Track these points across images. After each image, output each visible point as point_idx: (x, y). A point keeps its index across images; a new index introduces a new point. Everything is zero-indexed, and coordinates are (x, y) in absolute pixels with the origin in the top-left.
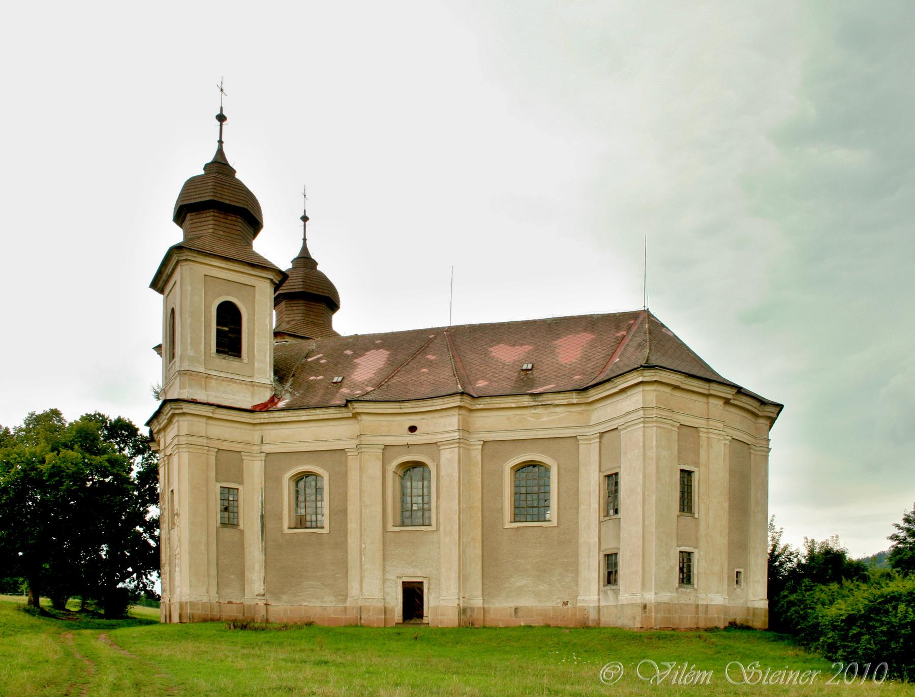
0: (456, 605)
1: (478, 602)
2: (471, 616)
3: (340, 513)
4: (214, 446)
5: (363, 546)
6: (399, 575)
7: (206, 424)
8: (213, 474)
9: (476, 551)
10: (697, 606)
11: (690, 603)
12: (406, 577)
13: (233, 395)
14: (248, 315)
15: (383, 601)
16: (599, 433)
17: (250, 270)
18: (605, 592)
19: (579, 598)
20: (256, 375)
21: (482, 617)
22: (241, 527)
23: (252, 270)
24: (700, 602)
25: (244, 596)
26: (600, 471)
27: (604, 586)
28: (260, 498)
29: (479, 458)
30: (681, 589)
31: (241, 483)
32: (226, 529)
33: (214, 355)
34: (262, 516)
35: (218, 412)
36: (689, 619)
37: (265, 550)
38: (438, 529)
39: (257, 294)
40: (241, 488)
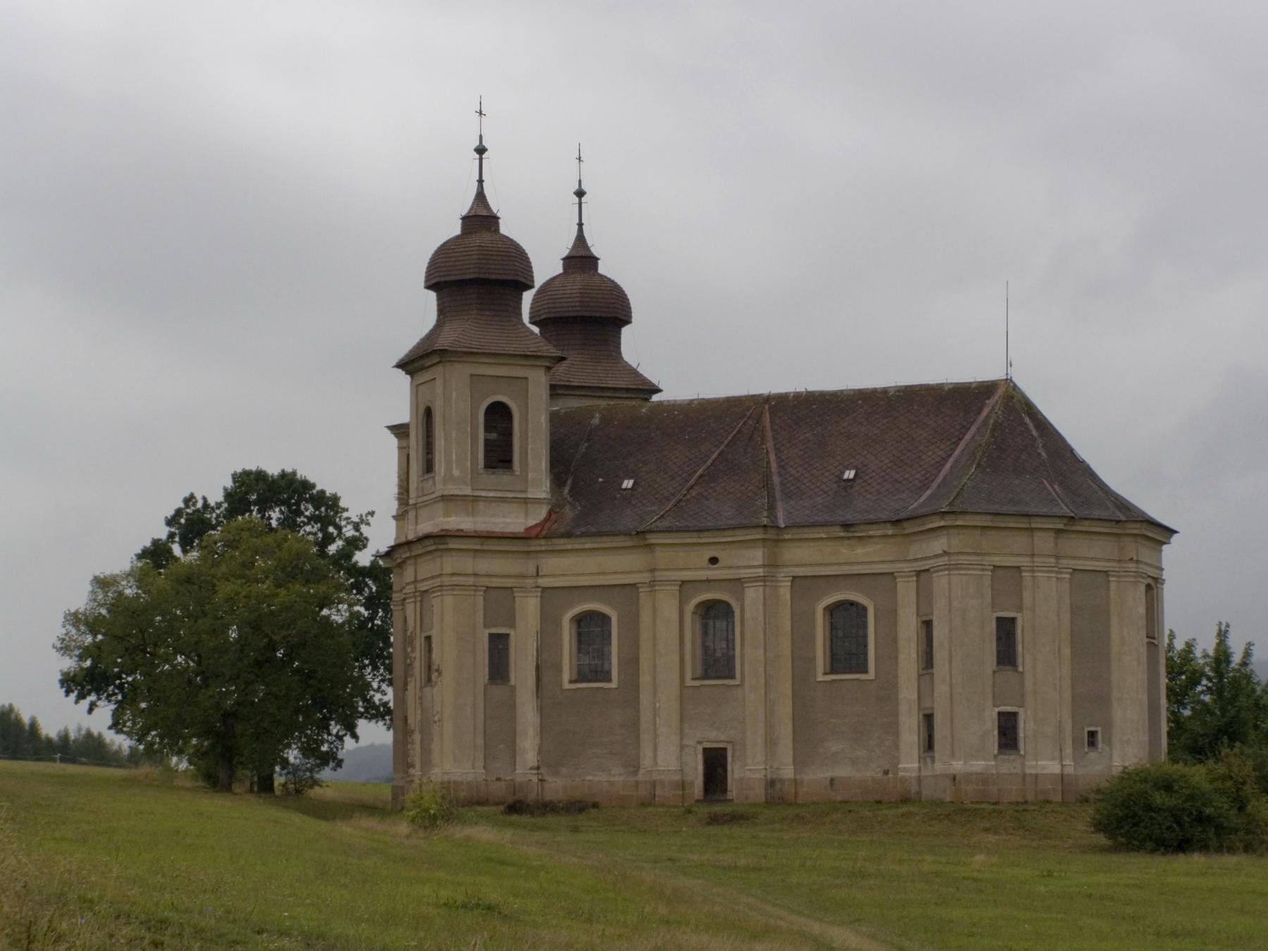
0: (763, 777)
1: (788, 772)
2: (781, 790)
3: (632, 663)
4: (482, 584)
5: (658, 705)
8: (480, 617)
9: (785, 711)
10: (1024, 775)
12: (708, 742)
13: (504, 517)
15: (680, 772)
16: (915, 571)
18: (925, 759)
19: (900, 766)
20: (530, 490)
21: (793, 791)
22: (512, 682)
24: (1028, 771)
25: (515, 770)
26: (918, 615)
27: (924, 752)
28: (535, 645)
29: (788, 596)
30: (1002, 756)
32: (494, 686)
33: (482, 471)
34: (538, 668)
37: (541, 710)
38: (741, 685)
39: (530, 387)
40: (512, 633)
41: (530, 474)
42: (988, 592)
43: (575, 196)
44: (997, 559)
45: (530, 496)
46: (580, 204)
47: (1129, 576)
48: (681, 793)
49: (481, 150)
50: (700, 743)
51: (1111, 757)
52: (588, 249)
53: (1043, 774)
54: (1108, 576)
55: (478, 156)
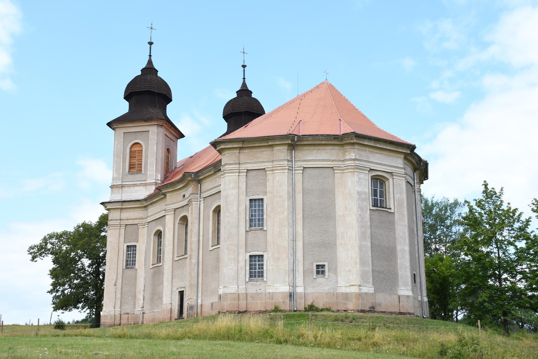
6: (177, 287)
7: (121, 212)
8: (122, 239)
11: (260, 292)
13: (136, 193)
14: (145, 147)
17: (145, 123)
23: (147, 123)
31: (137, 242)
33: (127, 174)
35: (124, 205)
36: (259, 304)
39: (150, 136)
41: (148, 173)
42: (243, 186)
43: (242, 67)
44: (249, 165)
45: (147, 182)
46: (244, 70)
47: (348, 169)
48: (170, 315)
49: (151, 43)
50: (177, 289)
51: (337, 282)
52: (153, 65)
53: (277, 293)
54: (334, 170)
55: (149, 46)
